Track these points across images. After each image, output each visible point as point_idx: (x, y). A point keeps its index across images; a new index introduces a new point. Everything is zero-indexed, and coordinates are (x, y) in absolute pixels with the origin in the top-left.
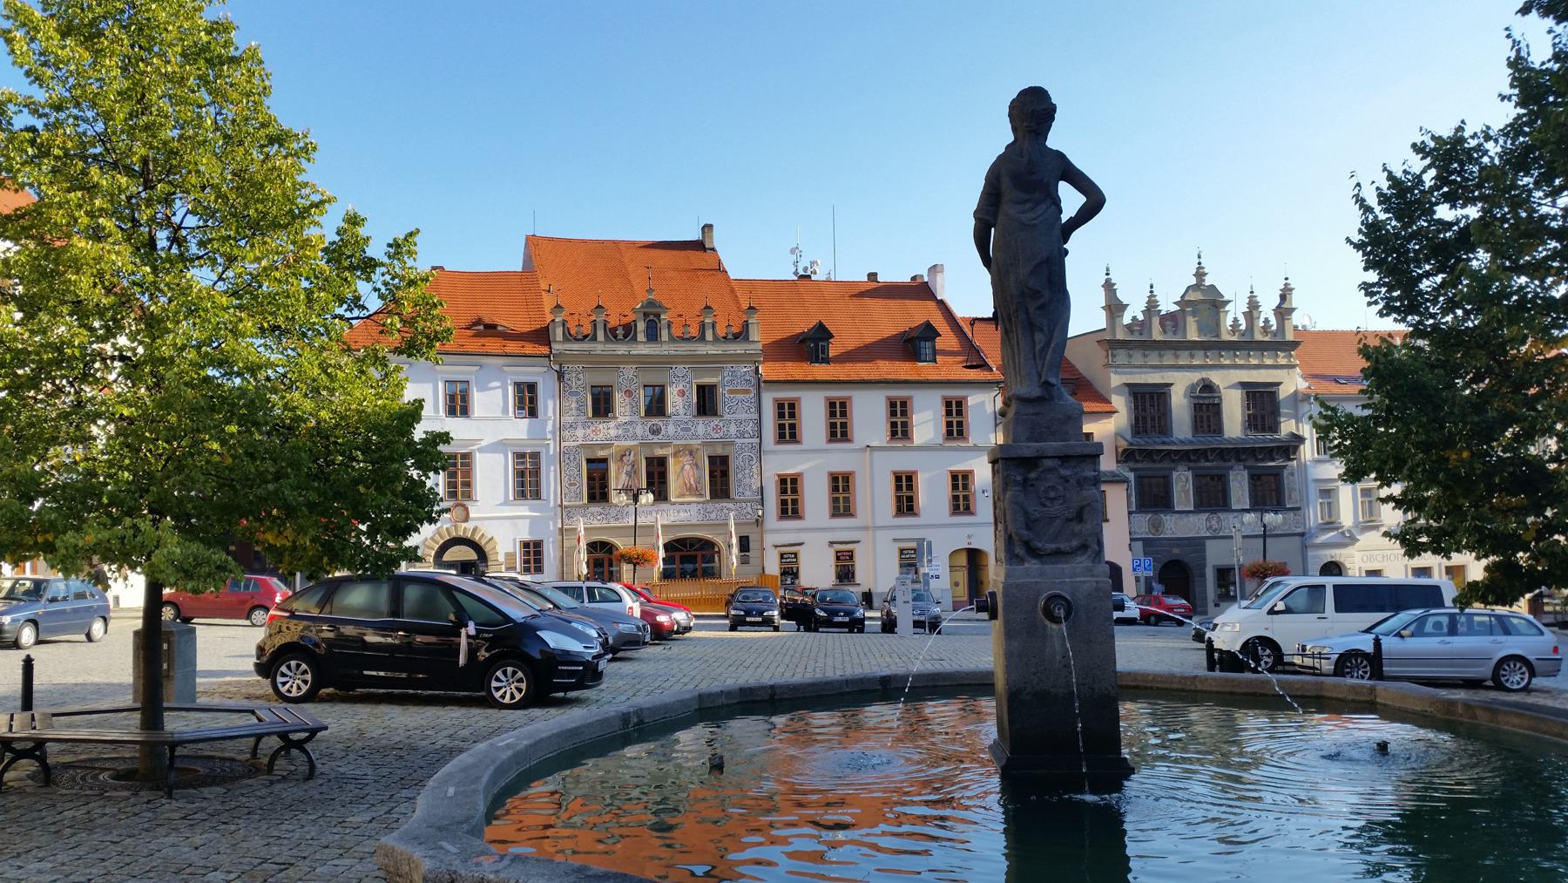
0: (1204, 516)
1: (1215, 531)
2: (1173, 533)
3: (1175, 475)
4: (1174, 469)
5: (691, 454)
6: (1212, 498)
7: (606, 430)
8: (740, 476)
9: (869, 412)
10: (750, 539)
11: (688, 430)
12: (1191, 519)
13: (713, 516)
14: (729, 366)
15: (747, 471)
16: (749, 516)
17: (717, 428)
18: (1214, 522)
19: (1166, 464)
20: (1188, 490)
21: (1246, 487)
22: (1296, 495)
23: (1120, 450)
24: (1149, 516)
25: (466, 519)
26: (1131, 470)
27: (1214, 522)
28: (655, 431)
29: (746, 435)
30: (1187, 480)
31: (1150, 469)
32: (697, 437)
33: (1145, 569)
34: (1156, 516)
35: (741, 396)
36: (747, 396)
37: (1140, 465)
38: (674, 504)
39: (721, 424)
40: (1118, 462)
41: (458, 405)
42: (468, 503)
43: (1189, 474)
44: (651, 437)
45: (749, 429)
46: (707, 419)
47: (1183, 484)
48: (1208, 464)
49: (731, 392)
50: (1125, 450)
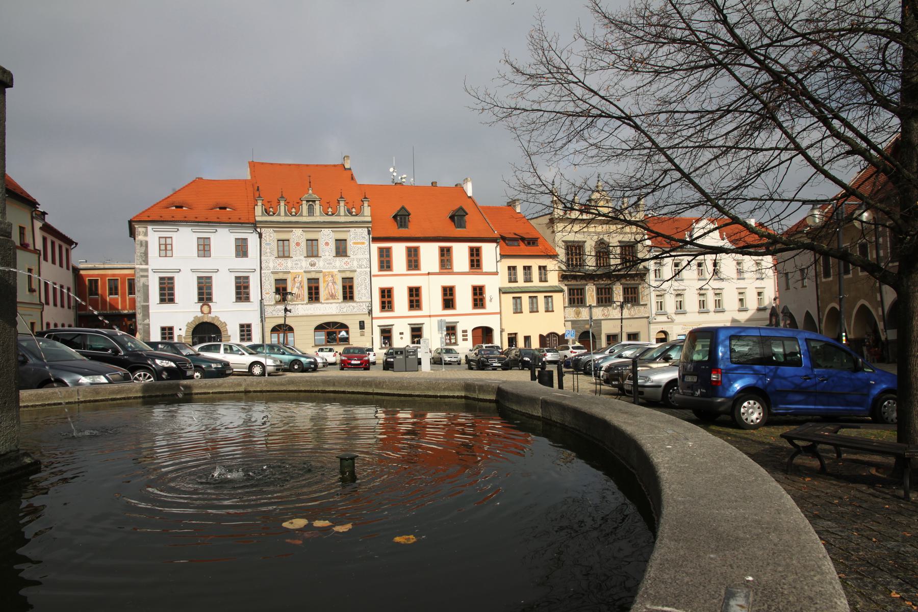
3: (587, 287)
4: (587, 284)
5: (332, 276)
6: (605, 299)
7: (287, 264)
8: (359, 288)
9: (429, 253)
10: (365, 322)
11: (331, 264)
13: (345, 310)
15: (363, 286)
16: (364, 310)
17: (347, 263)
18: (606, 312)
19: (583, 282)
21: (621, 294)
22: (645, 298)
24: (574, 309)
25: (210, 313)
26: (566, 285)
27: (606, 312)
28: (313, 265)
31: (575, 285)
32: (335, 267)
33: (571, 336)
35: (360, 246)
36: (363, 245)
37: (570, 283)
38: (323, 303)
39: (349, 261)
40: (559, 281)
41: (204, 248)
42: (210, 304)
44: (310, 267)
45: (364, 263)
46: (341, 258)
47: (591, 293)
48: (603, 282)
49: (354, 243)
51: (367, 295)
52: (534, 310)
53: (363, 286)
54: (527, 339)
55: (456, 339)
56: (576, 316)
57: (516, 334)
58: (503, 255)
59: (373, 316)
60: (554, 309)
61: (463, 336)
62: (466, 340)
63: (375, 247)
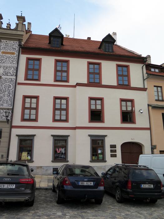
14: (5, 41)
15: (6, 93)
29: (9, 74)
35: (9, 55)
36: (13, 55)
45: (11, 71)
51: (10, 103)
53: (6, 93)
55: (103, 153)
59: (13, 125)
61: (111, 151)
62: (115, 156)
63: (23, 58)
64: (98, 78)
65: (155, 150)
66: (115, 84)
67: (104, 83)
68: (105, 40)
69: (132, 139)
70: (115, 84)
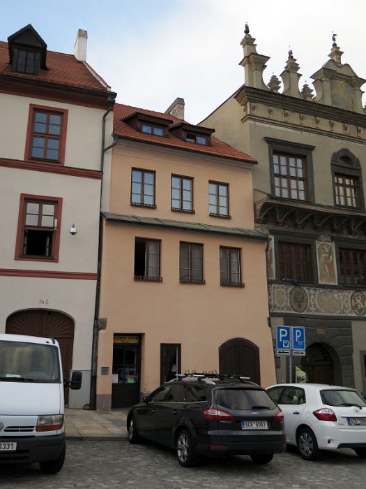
0: (349, 294)
1: (360, 311)
2: (317, 310)
3: (318, 244)
4: (316, 237)
12: (336, 295)
18: (359, 301)
19: (308, 230)
20: (332, 263)
23: (259, 207)
27: (359, 301)
30: (330, 252)
33: (296, 344)
34: (298, 289)
40: (256, 221)
43: (333, 245)
50: (266, 205)
52: (191, 276)
54: (171, 354)
56: (295, 307)
57: (140, 336)
58: (121, 137)
60: (245, 281)
64: (57, 148)
65: (101, 332)
66: (20, 155)
67: (69, 162)
68: (17, 41)
69: (43, 302)
70: (20, 155)
